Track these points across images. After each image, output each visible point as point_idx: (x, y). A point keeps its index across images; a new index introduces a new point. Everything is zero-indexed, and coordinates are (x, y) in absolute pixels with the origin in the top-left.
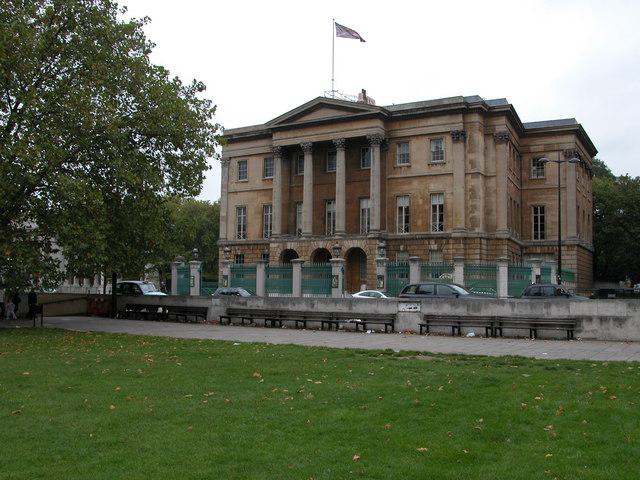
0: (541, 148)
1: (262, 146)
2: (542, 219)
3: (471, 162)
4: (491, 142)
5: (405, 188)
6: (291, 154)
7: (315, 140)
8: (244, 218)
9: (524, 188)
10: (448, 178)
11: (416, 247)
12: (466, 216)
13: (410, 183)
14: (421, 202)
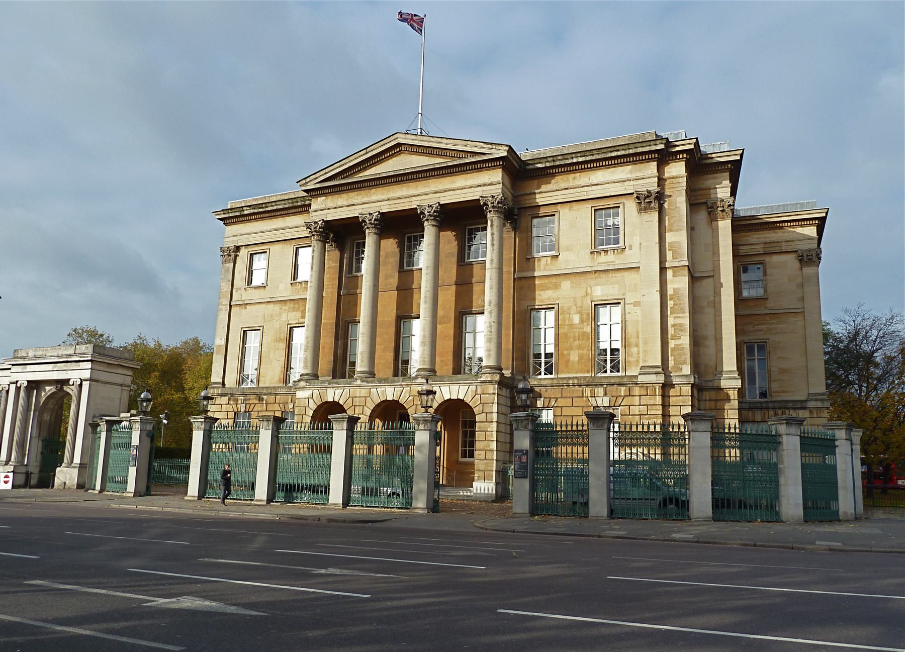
0: (760, 249)
1: (295, 224)
7: (386, 208)
10: (628, 276)
11: (568, 402)
13: (556, 287)
14: (576, 319)
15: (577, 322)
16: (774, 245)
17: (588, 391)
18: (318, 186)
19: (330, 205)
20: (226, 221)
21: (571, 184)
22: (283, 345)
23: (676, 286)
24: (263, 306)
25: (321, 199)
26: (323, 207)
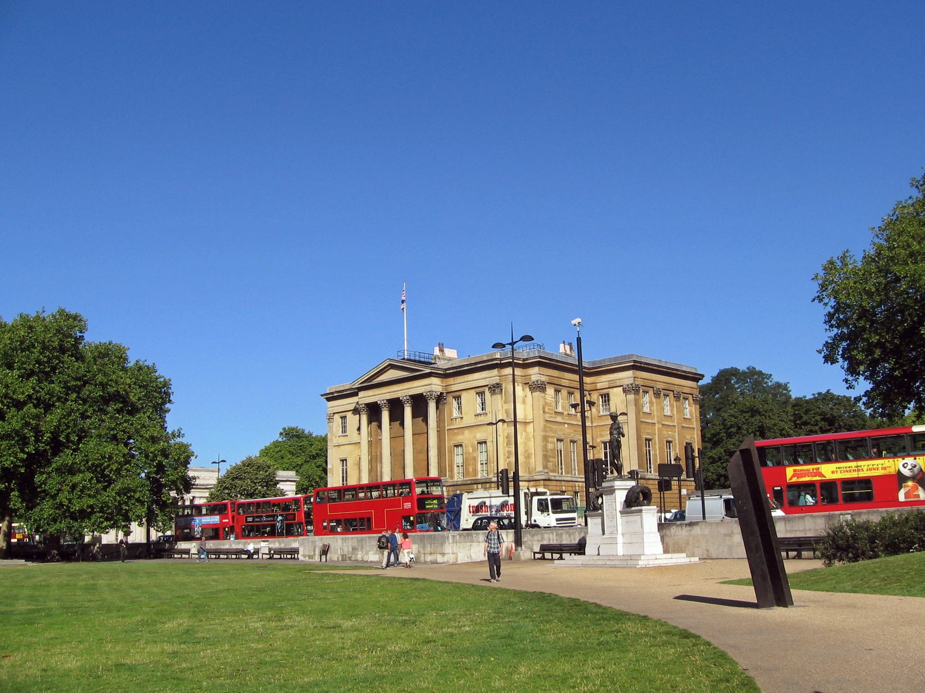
0: (606, 385)
5: (459, 439)
6: (373, 411)
7: (389, 397)
8: (346, 469)
9: (593, 425)
13: (463, 433)
15: (471, 451)
16: (613, 382)
17: (475, 486)
18: (360, 386)
19: (366, 395)
20: (329, 400)
21: (466, 380)
22: (357, 467)
24: (347, 446)
25: (362, 392)
26: (363, 396)
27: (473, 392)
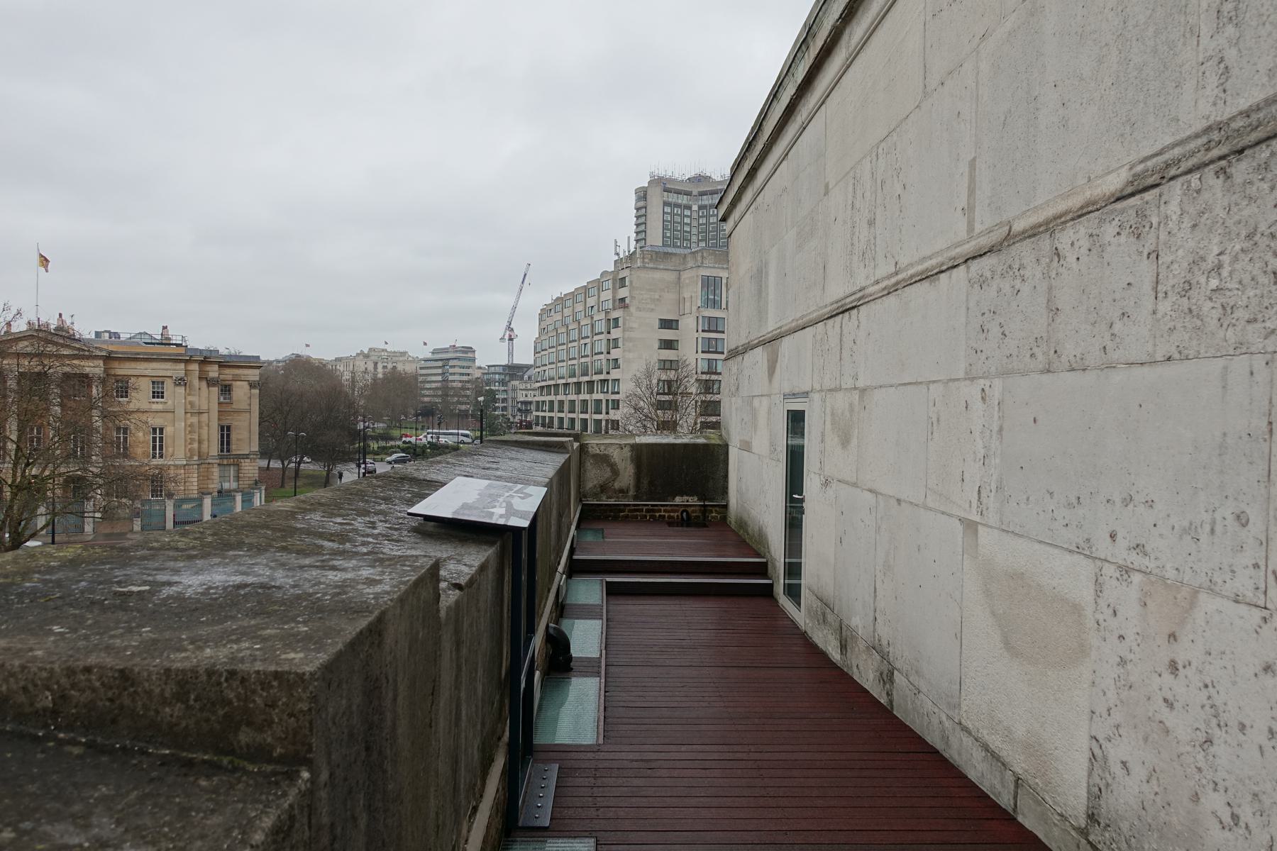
0: (230, 377)
2: (228, 436)
3: (191, 403)
4: (204, 384)
12: (185, 446)
23: (191, 420)
27: (148, 378)
